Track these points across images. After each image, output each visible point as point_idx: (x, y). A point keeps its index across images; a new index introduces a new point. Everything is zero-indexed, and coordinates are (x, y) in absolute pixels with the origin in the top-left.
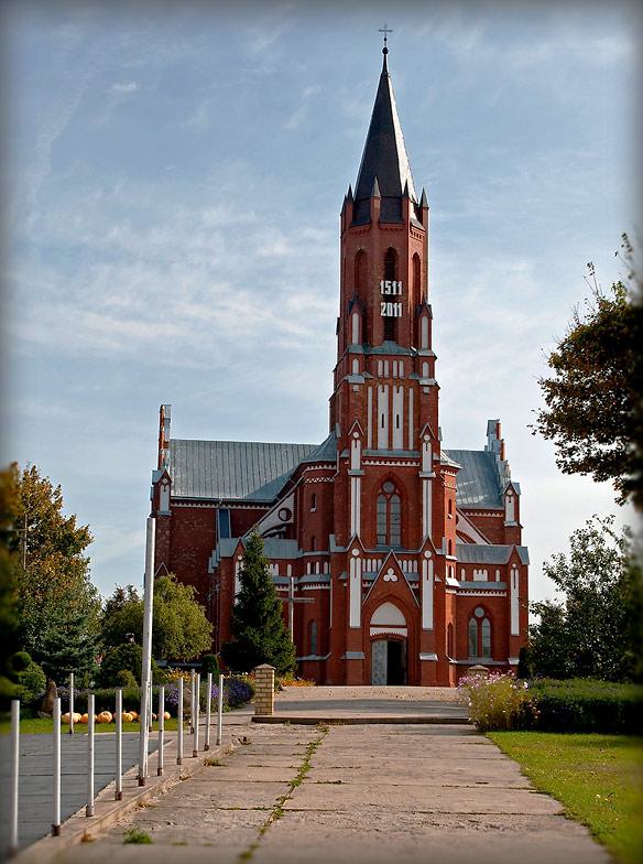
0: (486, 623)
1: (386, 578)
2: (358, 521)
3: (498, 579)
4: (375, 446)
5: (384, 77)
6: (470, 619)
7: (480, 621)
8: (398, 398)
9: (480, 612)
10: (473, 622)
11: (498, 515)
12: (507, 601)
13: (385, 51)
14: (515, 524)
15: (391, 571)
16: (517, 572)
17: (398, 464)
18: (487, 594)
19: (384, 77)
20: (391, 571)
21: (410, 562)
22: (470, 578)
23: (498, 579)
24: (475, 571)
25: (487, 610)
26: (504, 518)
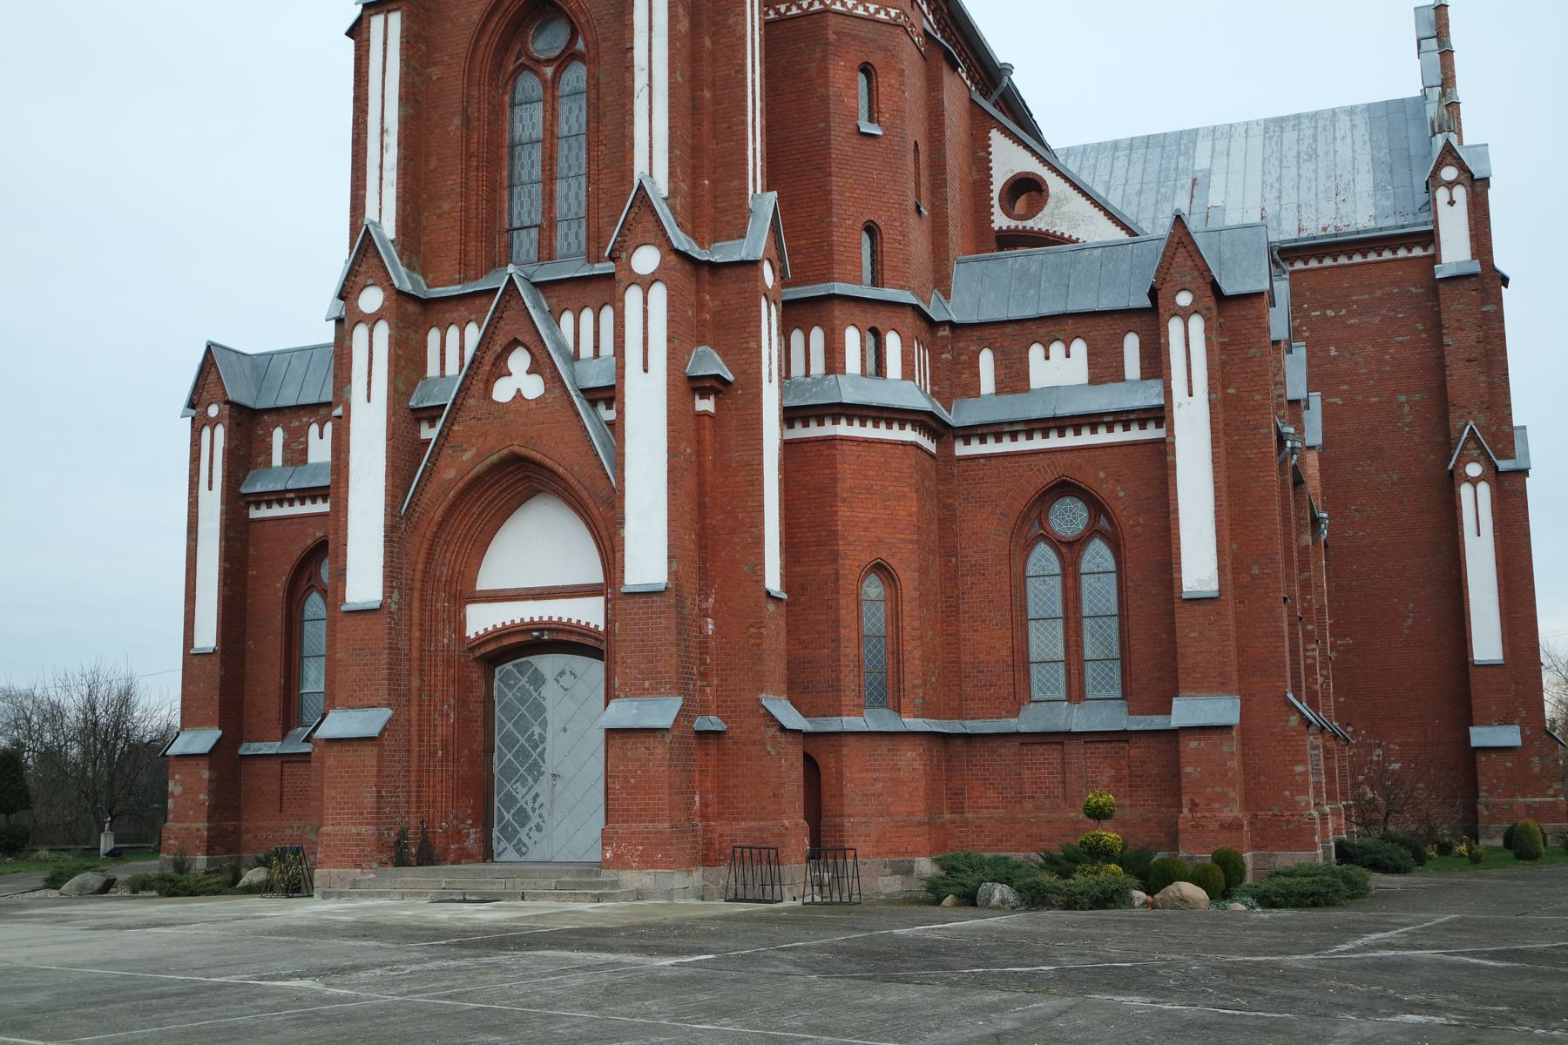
0: (1098, 556)
1: (503, 391)
2: (391, 175)
6: (1028, 547)
7: (1069, 551)
9: (1069, 517)
10: (1043, 559)
11: (1418, 252)
12: (1161, 456)
14: (1476, 267)
16: (1197, 324)
18: (1086, 438)
20: (519, 361)
21: (587, 316)
22: (1014, 378)
24: (1036, 351)
25: (1096, 506)
26: (1435, 259)
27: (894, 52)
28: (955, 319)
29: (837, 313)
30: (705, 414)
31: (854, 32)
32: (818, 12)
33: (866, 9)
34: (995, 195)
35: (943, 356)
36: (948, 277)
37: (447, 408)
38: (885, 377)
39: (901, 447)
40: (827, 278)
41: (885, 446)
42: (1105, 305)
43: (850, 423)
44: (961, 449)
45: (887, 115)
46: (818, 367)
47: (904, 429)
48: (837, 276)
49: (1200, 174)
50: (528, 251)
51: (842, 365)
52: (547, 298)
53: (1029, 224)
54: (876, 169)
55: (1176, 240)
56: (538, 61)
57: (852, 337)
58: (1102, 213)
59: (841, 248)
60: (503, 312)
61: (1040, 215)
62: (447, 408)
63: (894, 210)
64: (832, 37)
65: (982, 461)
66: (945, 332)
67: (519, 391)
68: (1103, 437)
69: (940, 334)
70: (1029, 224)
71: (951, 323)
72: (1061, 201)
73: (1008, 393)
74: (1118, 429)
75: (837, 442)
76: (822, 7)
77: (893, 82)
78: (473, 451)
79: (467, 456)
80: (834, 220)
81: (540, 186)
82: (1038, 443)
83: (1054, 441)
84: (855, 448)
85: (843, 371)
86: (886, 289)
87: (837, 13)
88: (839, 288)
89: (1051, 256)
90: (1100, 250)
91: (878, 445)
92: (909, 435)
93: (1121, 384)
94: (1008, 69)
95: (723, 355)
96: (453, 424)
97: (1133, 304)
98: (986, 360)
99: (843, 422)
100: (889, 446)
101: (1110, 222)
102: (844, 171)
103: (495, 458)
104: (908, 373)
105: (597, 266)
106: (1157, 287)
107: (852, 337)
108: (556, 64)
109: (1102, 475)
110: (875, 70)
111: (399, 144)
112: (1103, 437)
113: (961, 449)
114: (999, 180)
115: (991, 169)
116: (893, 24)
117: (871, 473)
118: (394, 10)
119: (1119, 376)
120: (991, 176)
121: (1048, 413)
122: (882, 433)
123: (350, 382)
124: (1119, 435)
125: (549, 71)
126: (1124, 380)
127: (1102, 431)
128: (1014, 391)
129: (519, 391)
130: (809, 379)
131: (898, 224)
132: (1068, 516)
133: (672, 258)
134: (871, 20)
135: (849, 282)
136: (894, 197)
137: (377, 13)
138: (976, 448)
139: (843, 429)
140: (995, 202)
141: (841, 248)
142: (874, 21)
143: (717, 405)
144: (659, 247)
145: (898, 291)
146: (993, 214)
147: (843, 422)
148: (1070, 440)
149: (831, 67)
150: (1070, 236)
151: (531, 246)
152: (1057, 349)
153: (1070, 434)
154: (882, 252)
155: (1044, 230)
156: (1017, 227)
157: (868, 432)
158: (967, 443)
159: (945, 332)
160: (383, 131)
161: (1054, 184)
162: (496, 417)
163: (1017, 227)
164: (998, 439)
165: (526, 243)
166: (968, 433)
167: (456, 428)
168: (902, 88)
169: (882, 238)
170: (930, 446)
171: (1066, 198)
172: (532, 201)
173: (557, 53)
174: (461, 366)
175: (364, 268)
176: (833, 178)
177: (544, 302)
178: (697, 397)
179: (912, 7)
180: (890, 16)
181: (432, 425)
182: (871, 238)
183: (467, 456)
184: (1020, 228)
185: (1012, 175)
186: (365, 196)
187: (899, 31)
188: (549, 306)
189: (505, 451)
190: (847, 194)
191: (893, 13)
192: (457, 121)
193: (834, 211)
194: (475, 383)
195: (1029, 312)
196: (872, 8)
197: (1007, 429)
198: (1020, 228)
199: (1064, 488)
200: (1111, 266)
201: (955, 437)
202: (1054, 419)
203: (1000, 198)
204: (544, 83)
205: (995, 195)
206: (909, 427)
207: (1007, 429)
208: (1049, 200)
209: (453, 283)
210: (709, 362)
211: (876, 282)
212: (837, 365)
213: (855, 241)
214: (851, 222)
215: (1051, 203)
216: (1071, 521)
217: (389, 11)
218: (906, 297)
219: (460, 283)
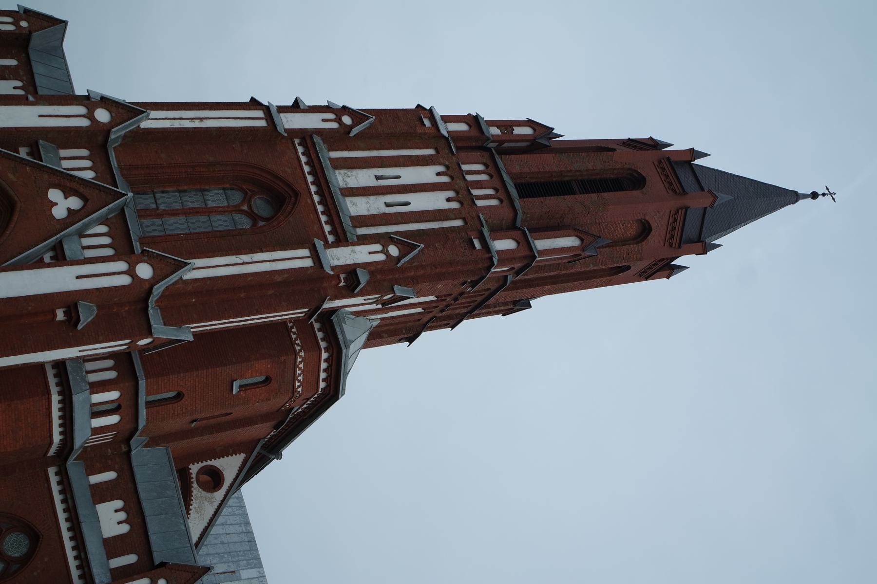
1: (54, 195)
2: (177, 124)
3: (117, 562)
4: (339, 164)
5: (793, 197)
8: (437, 201)
13: (814, 195)
15: (75, 203)
17: (320, 208)
18: (68, 545)
19: (793, 197)
20: (75, 203)
21: (107, 240)
22: (102, 494)
23: (117, 562)
24: (119, 504)
25: (25, 560)
27: (279, 393)
28: (133, 452)
29: (127, 384)
30: (55, 315)
31: (286, 370)
32: (294, 349)
33: (299, 375)
34: (209, 463)
35: (109, 450)
36: (157, 445)
37: (40, 163)
38: (92, 418)
39: (48, 434)
40: (147, 377)
41: (48, 425)
42: (153, 538)
43: (60, 402)
44: (52, 471)
45: (244, 395)
46: (92, 378)
47: (60, 435)
48: (149, 381)
49: (237, 574)
50: (143, 203)
51: (96, 392)
52: (115, 216)
53: (195, 485)
54: (213, 394)
55: (196, 571)
56: (250, 201)
57: (114, 395)
58: (206, 525)
59: (165, 381)
60: (104, 191)
61: (201, 490)
62: (40, 163)
63: (191, 407)
64: (282, 359)
65: (46, 485)
66: (124, 448)
67: (56, 204)
68: (70, 554)
69: (122, 445)
70: (195, 485)
71: (130, 451)
72: (210, 500)
73: (91, 492)
74: (77, 563)
75: (47, 396)
76: (298, 351)
77: (263, 395)
78: (14, 179)
79: (11, 176)
80: (182, 375)
81: (180, 207)
82: (62, 516)
83: (64, 525)
84: (44, 407)
85: (92, 393)
86: (145, 410)
87: (296, 359)
88: (142, 383)
89: (177, 501)
90: (184, 528)
91: (48, 420)
92: (57, 438)
93: (105, 559)
94: (279, 456)
95: (93, 321)
96: (30, 166)
97: (155, 555)
98: (111, 475)
99: (60, 398)
100: (48, 427)
101: (202, 530)
102: (210, 375)
103: (11, 192)
104: (96, 431)
105: (138, 243)
106: (167, 566)
107: (114, 395)
108: (249, 211)
109: (46, 559)
110: (268, 384)
111: (195, 128)
112: (70, 554)
113: (52, 471)
114: (217, 463)
115: (223, 457)
116: (294, 390)
117: (29, 419)
118: (267, 123)
119: (111, 555)
120: (219, 458)
121: (82, 519)
122: (56, 421)
123: (50, 105)
124: (73, 563)
125: (245, 208)
126: (108, 559)
127: (75, 553)
128: (93, 495)
129: (56, 204)
130: (84, 373)
131: (184, 411)
132: (16, 545)
133: (147, 286)
134: (294, 378)
135: (147, 389)
136: (199, 406)
137: (265, 114)
138: (54, 479)
139: (55, 398)
140: (205, 463)
141: (165, 381)
142: (294, 380)
143: (60, 322)
144: (153, 278)
145: (145, 417)
146: (198, 463)
147: (60, 398)
148: (66, 535)
149: (267, 360)
150: (191, 510)
151: (146, 205)
152: (122, 516)
153: (70, 534)
154: (167, 404)
155: (192, 494)
156: (192, 478)
157: (56, 414)
158: (57, 474)
159: (124, 448)
160: (201, 119)
161: (219, 495)
162: (38, 192)
163: (192, 478)
164: (61, 492)
165: (147, 202)
166: (63, 474)
167: (28, 168)
168: (260, 401)
169: (174, 403)
170: (52, 451)
171: (212, 503)
172: (171, 204)
173: (256, 211)
174: (68, 169)
175: (121, 111)
176: (205, 371)
177: (113, 215)
178: (64, 309)
179: (304, 399)
180: (298, 388)
181: (28, 154)
182: (174, 397)
183: (11, 176)
184: (192, 480)
185: (221, 469)
186: (164, 110)
187: (290, 394)
188: (111, 218)
189: (16, 198)
190: (197, 380)
191: (300, 390)
192: (211, 159)
193: (187, 374)
194: (58, 178)
195: (142, 495)
196: (300, 378)
197: (69, 496)
198: (192, 480)
199: (35, 538)
200: (176, 536)
201: (59, 466)
202: (79, 523)
203: (207, 465)
204: (238, 206)
205: (209, 463)
206: (61, 437)
207: (69, 496)
208: (210, 494)
209: (118, 162)
210: (87, 315)
211: (148, 404)
212: (95, 389)
213: (171, 388)
214: (181, 384)
215: (209, 495)
216: (13, 547)
217: (266, 120)
218: (142, 423)
219: (118, 166)
